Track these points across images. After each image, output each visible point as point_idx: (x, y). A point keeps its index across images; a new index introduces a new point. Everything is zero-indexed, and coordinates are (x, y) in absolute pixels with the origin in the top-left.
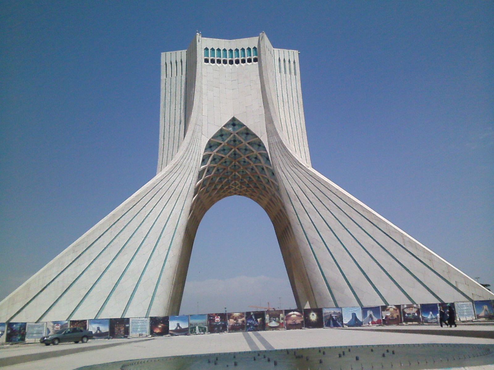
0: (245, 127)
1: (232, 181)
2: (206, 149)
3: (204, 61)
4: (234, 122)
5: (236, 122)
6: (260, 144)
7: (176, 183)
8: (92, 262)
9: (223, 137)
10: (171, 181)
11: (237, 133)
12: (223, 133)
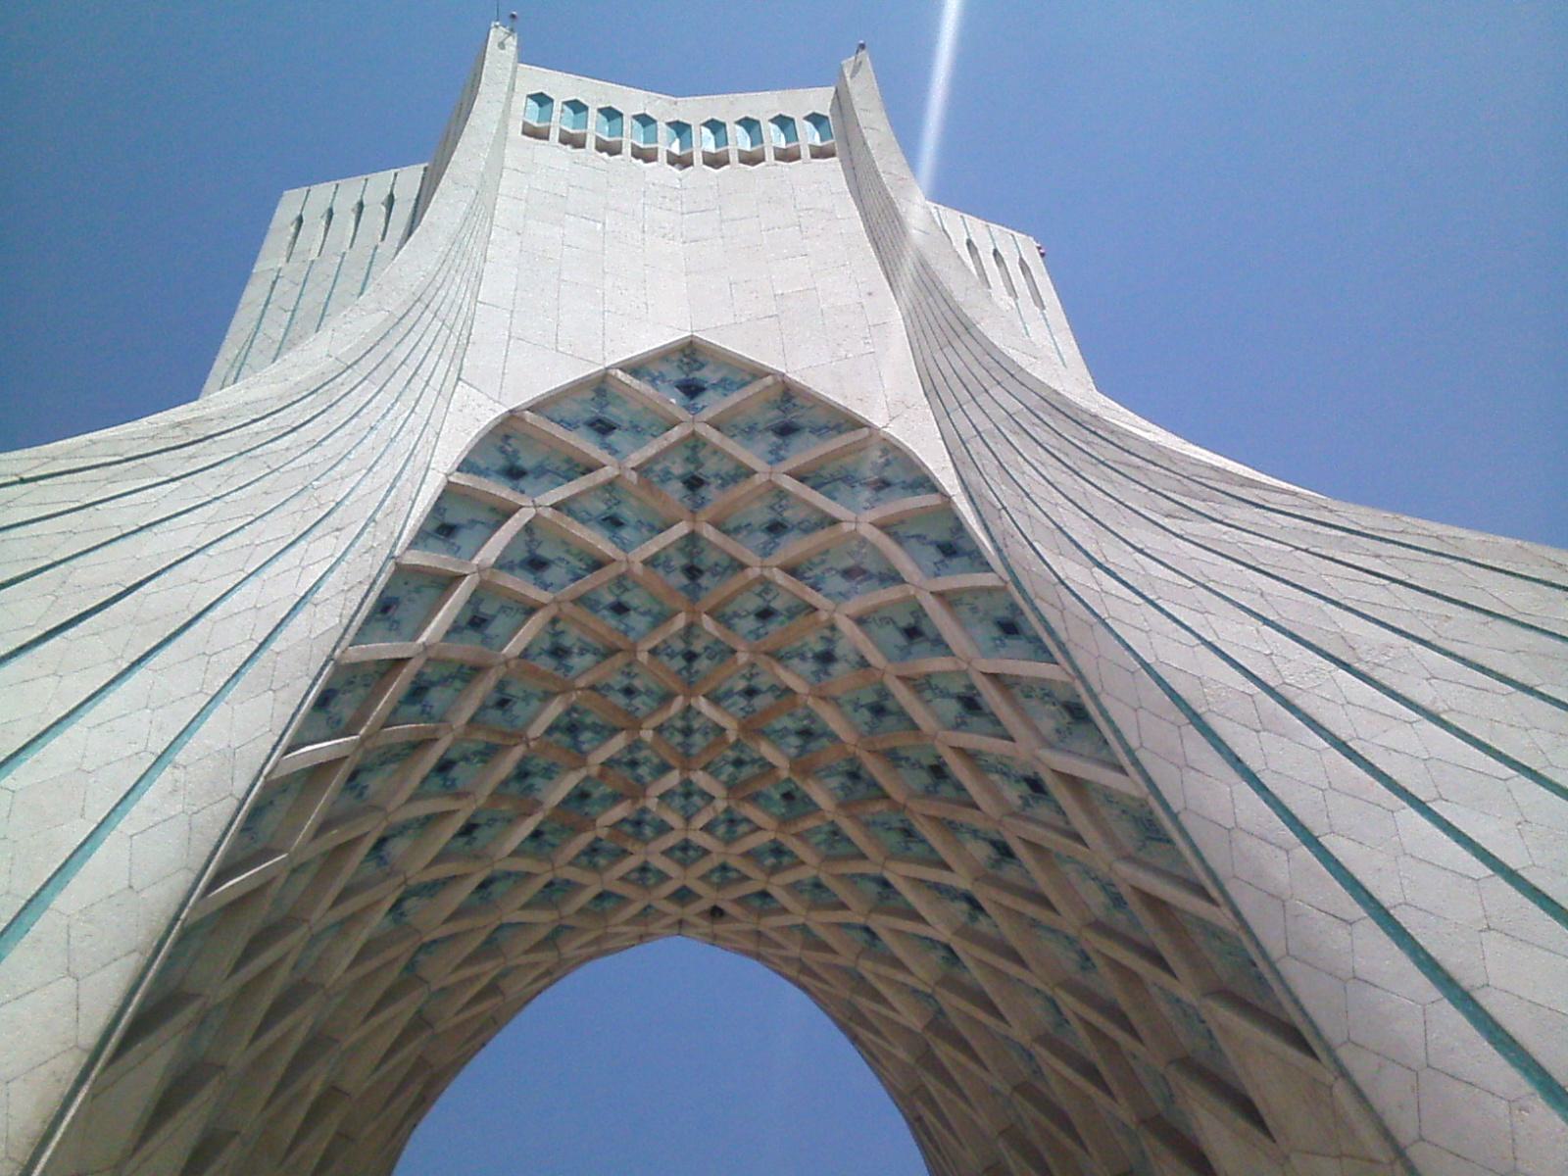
0: (769, 380)
1: (664, 768)
3: (515, 130)
5: (707, 375)
9: (613, 438)
12: (612, 413)
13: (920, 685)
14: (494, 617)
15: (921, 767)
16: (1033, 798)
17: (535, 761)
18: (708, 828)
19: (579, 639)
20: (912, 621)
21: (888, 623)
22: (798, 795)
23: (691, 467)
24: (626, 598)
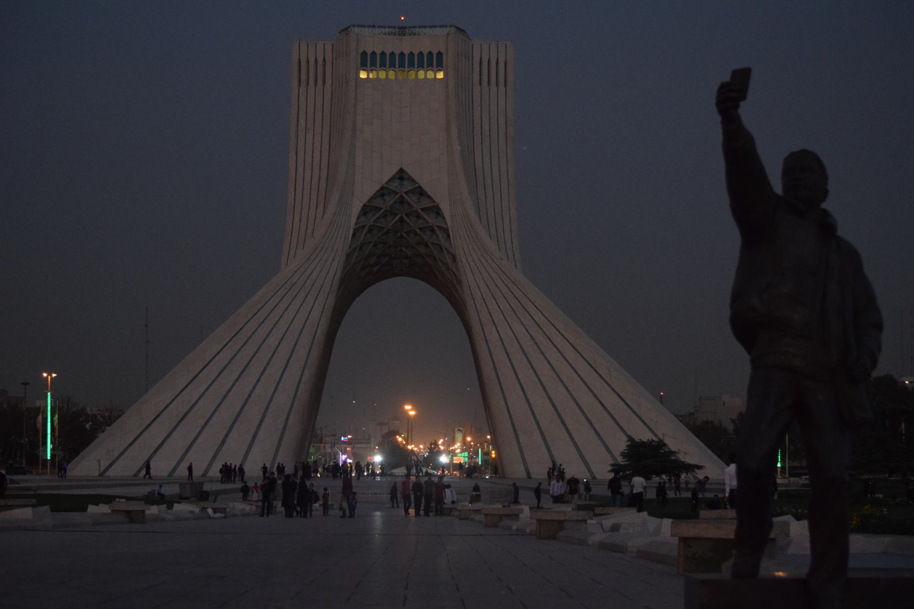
2: (358, 218)
4: (401, 175)
6: (437, 211)
7: (314, 274)
8: (210, 385)
9: (385, 197)
10: (308, 273)
11: (406, 193)
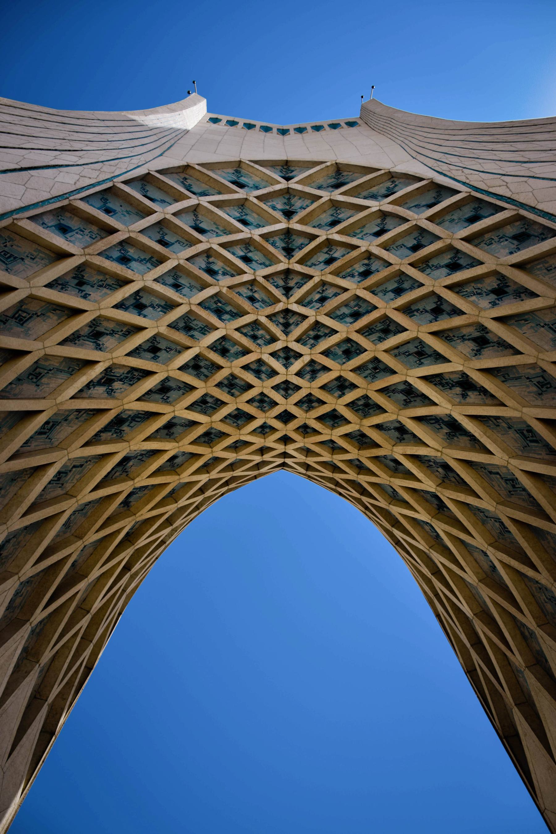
13: (423, 265)
14: (173, 244)
15: (426, 311)
16: (498, 299)
17: (195, 322)
18: (299, 374)
19: (223, 268)
20: (415, 242)
21: (401, 247)
22: (353, 349)
23: (288, 207)
24: (250, 255)
